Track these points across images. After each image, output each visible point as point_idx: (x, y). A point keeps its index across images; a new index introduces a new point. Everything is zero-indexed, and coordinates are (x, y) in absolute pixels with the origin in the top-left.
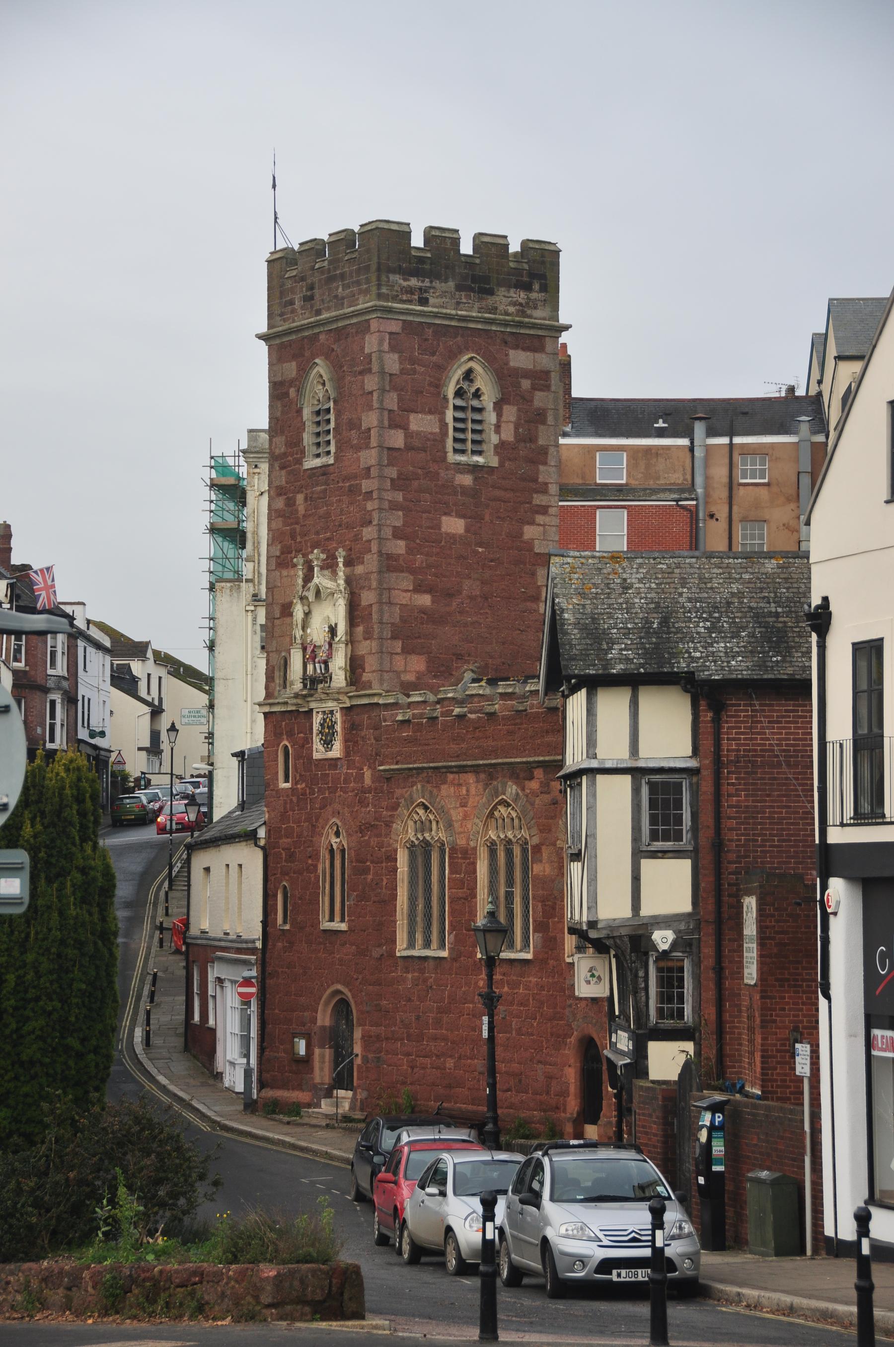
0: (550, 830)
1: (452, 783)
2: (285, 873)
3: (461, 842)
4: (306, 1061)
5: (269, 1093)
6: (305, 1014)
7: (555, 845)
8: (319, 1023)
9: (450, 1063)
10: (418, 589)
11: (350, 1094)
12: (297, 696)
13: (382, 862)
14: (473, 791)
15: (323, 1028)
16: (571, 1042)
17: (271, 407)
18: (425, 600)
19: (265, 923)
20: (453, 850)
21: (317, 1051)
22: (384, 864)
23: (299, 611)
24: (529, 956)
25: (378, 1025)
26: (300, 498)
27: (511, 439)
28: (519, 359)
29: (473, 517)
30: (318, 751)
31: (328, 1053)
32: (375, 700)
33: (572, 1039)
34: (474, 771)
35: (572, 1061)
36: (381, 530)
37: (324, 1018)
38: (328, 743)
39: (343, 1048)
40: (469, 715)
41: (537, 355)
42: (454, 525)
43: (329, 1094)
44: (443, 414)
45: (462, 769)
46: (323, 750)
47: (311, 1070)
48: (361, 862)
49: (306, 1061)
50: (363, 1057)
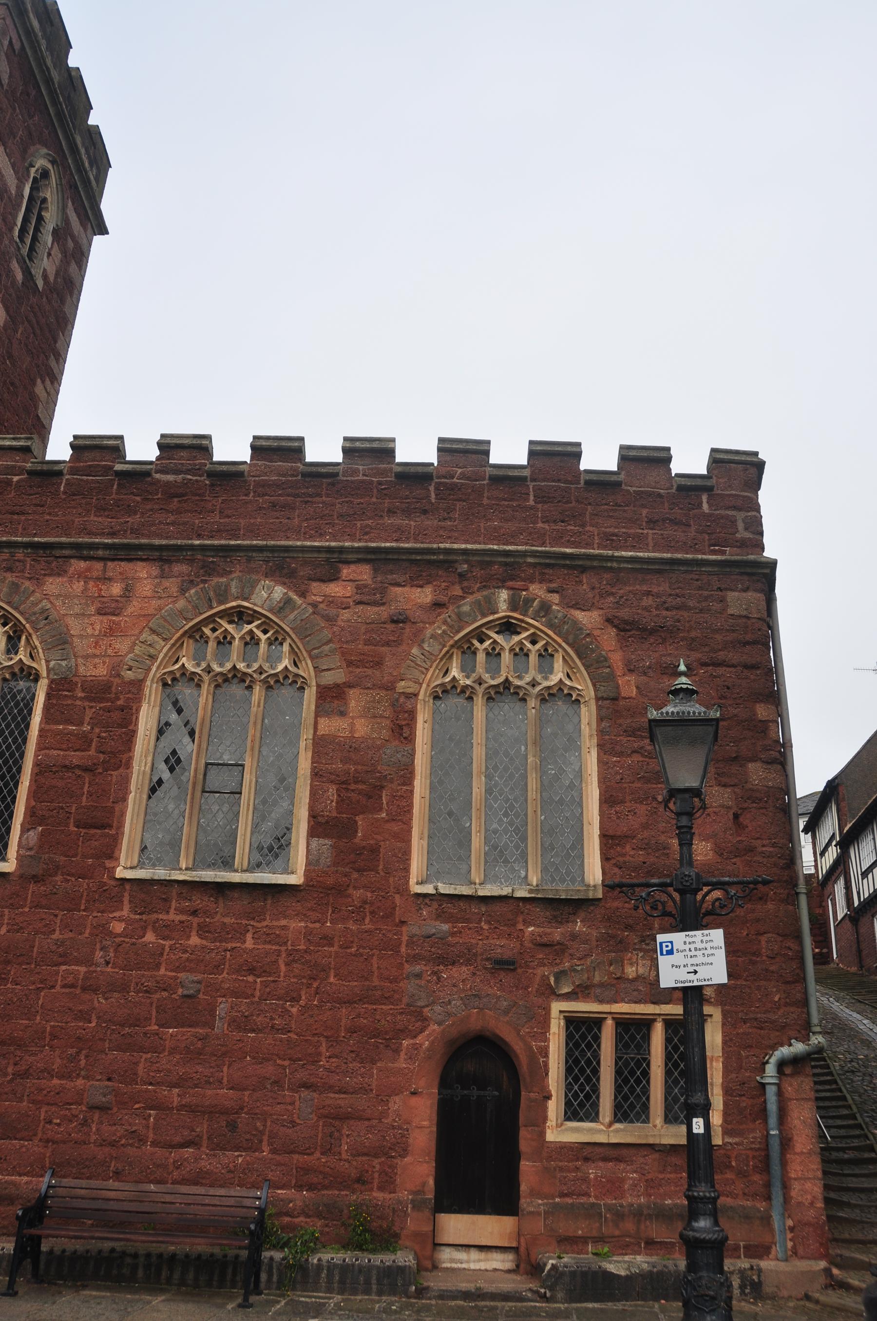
0: (378, 664)
1: (81, 575)
3: (101, 671)
7: (390, 687)
14: (145, 588)
16: (416, 1047)
33: (424, 1041)
35: (421, 1084)
40: (158, 476)
41: (81, 229)
45: (127, 553)
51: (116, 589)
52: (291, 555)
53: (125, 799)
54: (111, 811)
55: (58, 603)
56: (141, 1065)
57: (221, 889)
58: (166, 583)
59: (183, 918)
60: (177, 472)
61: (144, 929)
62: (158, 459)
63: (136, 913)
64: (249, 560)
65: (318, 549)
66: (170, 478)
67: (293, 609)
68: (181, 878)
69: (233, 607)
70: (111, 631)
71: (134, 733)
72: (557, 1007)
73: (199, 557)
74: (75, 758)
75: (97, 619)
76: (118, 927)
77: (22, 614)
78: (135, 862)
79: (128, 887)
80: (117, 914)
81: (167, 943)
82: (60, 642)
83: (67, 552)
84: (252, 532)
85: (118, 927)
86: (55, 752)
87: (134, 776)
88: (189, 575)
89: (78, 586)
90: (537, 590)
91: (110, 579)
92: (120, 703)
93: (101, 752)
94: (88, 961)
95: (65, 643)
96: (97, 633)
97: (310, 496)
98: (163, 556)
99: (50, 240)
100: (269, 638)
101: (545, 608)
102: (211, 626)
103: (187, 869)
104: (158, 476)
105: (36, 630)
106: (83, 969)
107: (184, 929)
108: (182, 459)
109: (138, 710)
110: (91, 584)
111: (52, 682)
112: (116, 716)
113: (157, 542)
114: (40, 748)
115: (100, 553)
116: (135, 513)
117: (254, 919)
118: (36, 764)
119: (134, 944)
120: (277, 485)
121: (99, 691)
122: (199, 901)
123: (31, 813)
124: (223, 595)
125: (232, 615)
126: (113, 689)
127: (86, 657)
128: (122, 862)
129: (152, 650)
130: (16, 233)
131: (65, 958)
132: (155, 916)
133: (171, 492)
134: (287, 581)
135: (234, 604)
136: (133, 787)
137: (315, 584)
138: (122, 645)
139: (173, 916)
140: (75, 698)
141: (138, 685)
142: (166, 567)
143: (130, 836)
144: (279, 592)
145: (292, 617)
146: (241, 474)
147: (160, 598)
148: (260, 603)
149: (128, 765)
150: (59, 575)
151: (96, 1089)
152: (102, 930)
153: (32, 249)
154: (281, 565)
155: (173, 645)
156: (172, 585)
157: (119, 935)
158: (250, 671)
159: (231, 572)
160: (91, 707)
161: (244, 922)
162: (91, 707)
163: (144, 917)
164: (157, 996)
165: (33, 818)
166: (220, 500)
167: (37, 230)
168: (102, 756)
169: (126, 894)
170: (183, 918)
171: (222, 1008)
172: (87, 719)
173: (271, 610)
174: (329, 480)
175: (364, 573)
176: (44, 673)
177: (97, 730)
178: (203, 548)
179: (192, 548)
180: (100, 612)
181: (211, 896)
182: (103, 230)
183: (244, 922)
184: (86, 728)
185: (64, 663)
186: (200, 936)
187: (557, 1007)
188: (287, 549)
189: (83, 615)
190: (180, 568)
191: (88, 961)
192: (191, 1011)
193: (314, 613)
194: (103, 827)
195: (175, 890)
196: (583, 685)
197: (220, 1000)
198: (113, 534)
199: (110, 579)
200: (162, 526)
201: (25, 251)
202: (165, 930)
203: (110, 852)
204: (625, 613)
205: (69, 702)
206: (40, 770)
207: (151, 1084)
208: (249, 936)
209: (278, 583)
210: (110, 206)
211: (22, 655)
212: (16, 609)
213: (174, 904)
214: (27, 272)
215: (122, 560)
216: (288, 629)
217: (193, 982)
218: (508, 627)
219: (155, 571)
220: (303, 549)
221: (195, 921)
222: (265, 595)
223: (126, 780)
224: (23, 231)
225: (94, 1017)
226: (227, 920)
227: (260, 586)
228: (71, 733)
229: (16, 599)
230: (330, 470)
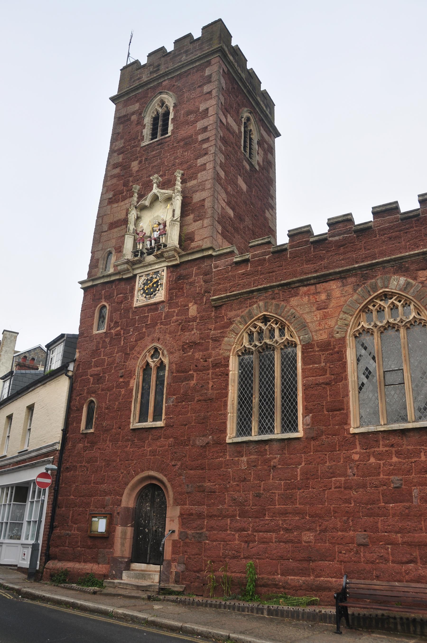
1: (305, 294)
2: (91, 392)
3: (324, 336)
5: (51, 564)
6: (107, 498)
8: (124, 504)
9: (308, 537)
10: (229, 204)
11: (157, 568)
12: (128, 262)
13: (208, 369)
14: (337, 293)
15: (127, 509)
18: (231, 213)
19: (65, 431)
20: (307, 347)
21: (119, 529)
22: (210, 371)
25: (200, 504)
30: (139, 300)
31: (130, 531)
32: (210, 252)
34: (341, 278)
36: (210, 163)
37: (128, 501)
38: (149, 292)
39: (145, 527)
40: (331, 239)
41: (269, 138)
43: (128, 568)
45: (324, 279)
46: (145, 299)
47: (112, 545)
48: (183, 372)
49: (107, 538)
50: (180, 533)
51: (323, 297)
52: (404, 260)
53: (348, 395)
54: (342, 402)
55: (298, 309)
56: (380, 524)
57: (404, 432)
58: (346, 288)
59: (387, 449)
60: (339, 235)
61: (369, 456)
62: (329, 231)
63: (363, 449)
64: (384, 268)
65: (418, 254)
66: (337, 238)
67: (412, 287)
68: (382, 429)
69: (381, 293)
70: (325, 317)
71: (345, 363)
73: (359, 272)
74: (321, 379)
75: (317, 312)
76: (356, 457)
77: (283, 317)
78: (358, 425)
79: (357, 437)
80: (354, 451)
81: (382, 462)
82: (303, 326)
83: (297, 285)
84: (382, 254)
85: (356, 457)
86: (311, 378)
87: (350, 383)
88: (356, 282)
89: (306, 299)
91: (319, 293)
92: (336, 349)
93: (332, 375)
94: (345, 475)
95: (305, 326)
96: (319, 319)
97: (407, 229)
98: (342, 276)
99: (257, 147)
100: (402, 304)
102: (372, 304)
103: (384, 425)
104: (331, 239)
105: (291, 323)
106: (343, 479)
107: (389, 454)
108: (340, 228)
109: (345, 352)
110: (311, 296)
111: (303, 346)
112: (336, 356)
113: (337, 270)
114: (304, 377)
115: (312, 281)
116: (324, 259)
117: (423, 445)
118: (304, 385)
119: (365, 464)
120: (390, 228)
121: (325, 346)
122: (393, 440)
123: (305, 408)
124: (375, 288)
125: (381, 296)
126: (332, 344)
127: (316, 331)
128: (352, 425)
129: (346, 322)
130: (242, 149)
131: (334, 475)
132: (373, 450)
133: (339, 245)
134: (405, 274)
135: (381, 291)
136: (350, 389)
137: (420, 272)
138: (331, 322)
139: (382, 449)
140: (316, 351)
141: (343, 339)
142: (344, 281)
143: (353, 412)
144: (402, 280)
145: (412, 291)
146: (370, 227)
147: (345, 296)
148: (394, 288)
149: (346, 378)
150: (296, 296)
151: (360, 536)
152: (349, 459)
153: (250, 153)
154: (400, 266)
155: (356, 317)
156: (349, 289)
157: (357, 461)
158: (396, 322)
159: (376, 276)
160: (323, 354)
161: (418, 447)
162: (323, 354)
163: (368, 451)
164: (381, 488)
165: (307, 411)
166: (363, 242)
167: (250, 144)
168: (333, 376)
169: (357, 441)
170: (387, 449)
171: (415, 492)
172: (322, 360)
173: (400, 290)
174: (416, 219)
176: (298, 343)
177: (328, 365)
178: (360, 268)
179: (355, 269)
180: (318, 309)
181: (399, 436)
182: (278, 135)
183: (418, 447)
184: (323, 364)
185: (306, 336)
186: (397, 457)
188: (402, 258)
189: (311, 312)
190: (350, 280)
191: (345, 475)
192: (400, 495)
193: (423, 286)
194: (339, 410)
195: (380, 436)
197: (413, 488)
198: (316, 271)
199: (319, 293)
200: (338, 262)
201: (248, 156)
202: (379, 456)
203: (345, 421)
205: (313, 354)
206: (306, 388)
207: (386, 532)
208: (422, 454)
209: (401, 276)
210: (279, 123)
211: (287, 336)
212: (280, 316)
213: (381, 443)
214: (251, 165)
215: (323, 282)
216: (411, 297)
217: (398, 480)
219: (339, 284)
220: (410, 256)
221: (393, 450)
222: (396, 283)
223: (347, 386)
224: (245, 147)
225: (352, 501)
226: (409, 447)
227: (392, 280)
228: (316, 368)
229: (279, 311)
230: (415, 213)
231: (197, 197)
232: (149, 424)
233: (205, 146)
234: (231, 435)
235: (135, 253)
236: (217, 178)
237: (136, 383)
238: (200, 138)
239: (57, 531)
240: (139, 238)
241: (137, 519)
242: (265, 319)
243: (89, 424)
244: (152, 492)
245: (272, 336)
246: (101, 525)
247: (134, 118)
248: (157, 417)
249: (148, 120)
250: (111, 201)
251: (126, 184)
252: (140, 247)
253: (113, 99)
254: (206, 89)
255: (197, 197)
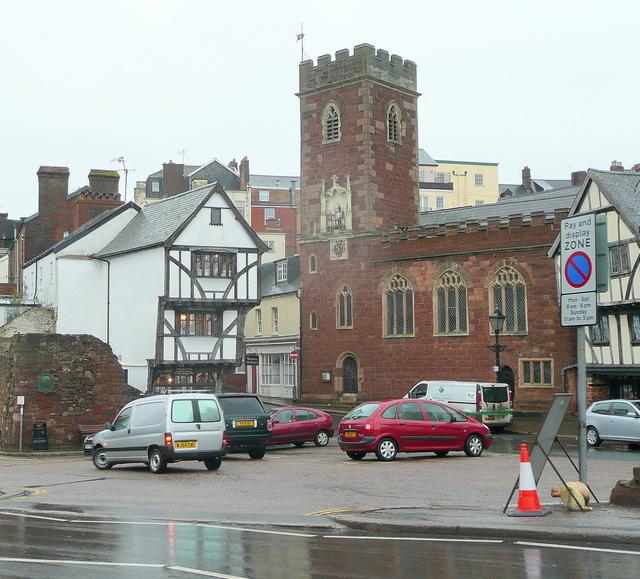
4: (331, 382)
17: (301, 122)
19: (301, 328)
21: (336, 378)
23: (323, 200)
24: (467, 334)
26: (320, 156)
27: (405, 135)
28: (407, 105)
29: (395, 164)
30: (333, 257)
31: (341, 379)
37: (339, 364)
38: (339, 253)
42: (389, 167)
44: (385, 122)
45: (423, 259)
47: (333, 386)
49: (331, 382)
70: (425, 279)
72: (520, 359)
82: (415, 283)
90: (512, 259)
101: (514, 263)
121: (424, 294)
138: (427, 282)
175: (474, 258)
187: (520, 359)
196: (523, 283)
203: (432, 331)
204: (533, 262)
218: (507, 269)
231: (361, 193)
232: (345, 327)
233: (363, 156)
234: (385, 334)
235: (328, 228)
236: (373, 180)
237: (337, 304)
238: (359, 148)
239: (304, 380)
240: (329, 217)
241: (345, 374)
242: (398, 277)
243: (314, 326)
244: (350, 361)
245: (402, 285)
246: (327, 377)
247: (314, 115)
248: (349, 324)
249: (324, 123)
250: (308, 184)
251: (316, 172)
252: (330, 224)
253: (297, 95)
254: (361, 108)
255: (361, 193)
